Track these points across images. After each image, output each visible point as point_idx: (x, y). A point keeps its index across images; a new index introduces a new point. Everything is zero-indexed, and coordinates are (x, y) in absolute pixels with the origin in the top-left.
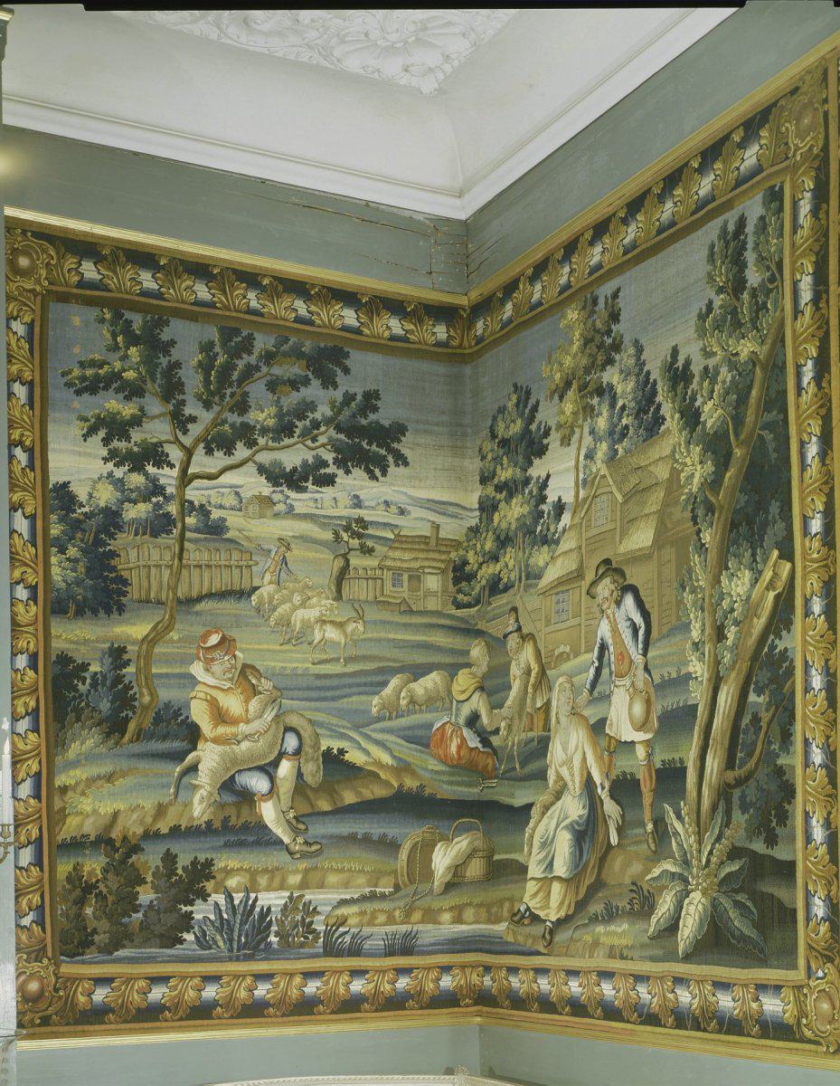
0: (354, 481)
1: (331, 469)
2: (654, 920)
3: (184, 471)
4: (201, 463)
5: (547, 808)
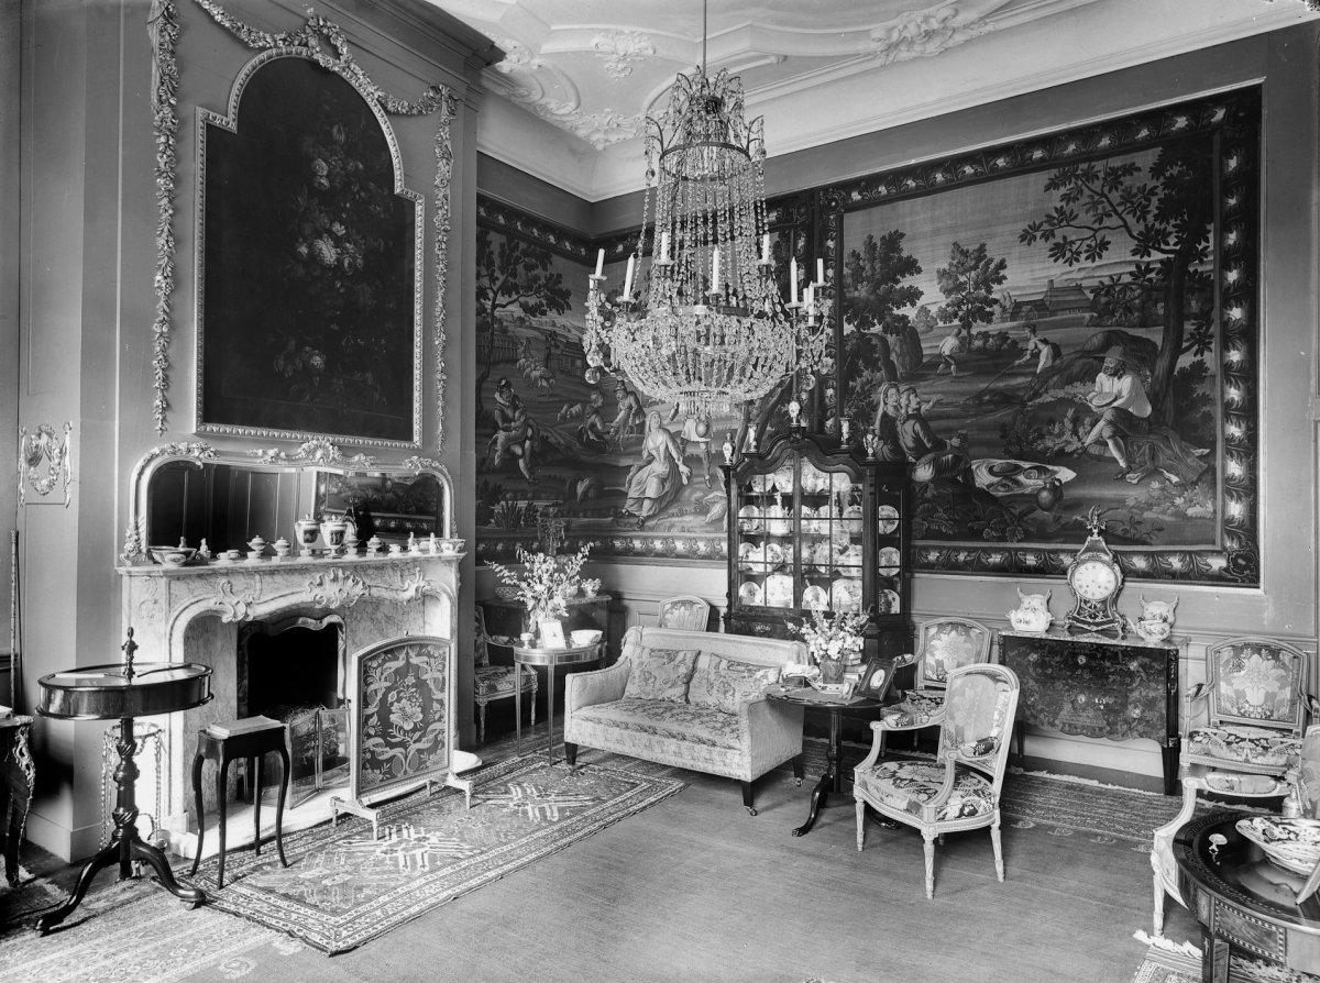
0: (552, 314)
1: (545, 308)
2: (709, 515)
3: (494, 303)
4: (501, 300)
5: (641, 468)
